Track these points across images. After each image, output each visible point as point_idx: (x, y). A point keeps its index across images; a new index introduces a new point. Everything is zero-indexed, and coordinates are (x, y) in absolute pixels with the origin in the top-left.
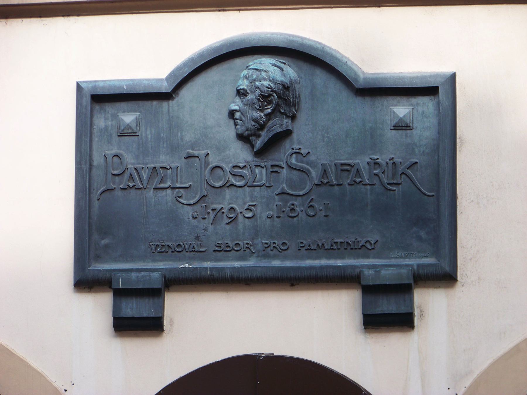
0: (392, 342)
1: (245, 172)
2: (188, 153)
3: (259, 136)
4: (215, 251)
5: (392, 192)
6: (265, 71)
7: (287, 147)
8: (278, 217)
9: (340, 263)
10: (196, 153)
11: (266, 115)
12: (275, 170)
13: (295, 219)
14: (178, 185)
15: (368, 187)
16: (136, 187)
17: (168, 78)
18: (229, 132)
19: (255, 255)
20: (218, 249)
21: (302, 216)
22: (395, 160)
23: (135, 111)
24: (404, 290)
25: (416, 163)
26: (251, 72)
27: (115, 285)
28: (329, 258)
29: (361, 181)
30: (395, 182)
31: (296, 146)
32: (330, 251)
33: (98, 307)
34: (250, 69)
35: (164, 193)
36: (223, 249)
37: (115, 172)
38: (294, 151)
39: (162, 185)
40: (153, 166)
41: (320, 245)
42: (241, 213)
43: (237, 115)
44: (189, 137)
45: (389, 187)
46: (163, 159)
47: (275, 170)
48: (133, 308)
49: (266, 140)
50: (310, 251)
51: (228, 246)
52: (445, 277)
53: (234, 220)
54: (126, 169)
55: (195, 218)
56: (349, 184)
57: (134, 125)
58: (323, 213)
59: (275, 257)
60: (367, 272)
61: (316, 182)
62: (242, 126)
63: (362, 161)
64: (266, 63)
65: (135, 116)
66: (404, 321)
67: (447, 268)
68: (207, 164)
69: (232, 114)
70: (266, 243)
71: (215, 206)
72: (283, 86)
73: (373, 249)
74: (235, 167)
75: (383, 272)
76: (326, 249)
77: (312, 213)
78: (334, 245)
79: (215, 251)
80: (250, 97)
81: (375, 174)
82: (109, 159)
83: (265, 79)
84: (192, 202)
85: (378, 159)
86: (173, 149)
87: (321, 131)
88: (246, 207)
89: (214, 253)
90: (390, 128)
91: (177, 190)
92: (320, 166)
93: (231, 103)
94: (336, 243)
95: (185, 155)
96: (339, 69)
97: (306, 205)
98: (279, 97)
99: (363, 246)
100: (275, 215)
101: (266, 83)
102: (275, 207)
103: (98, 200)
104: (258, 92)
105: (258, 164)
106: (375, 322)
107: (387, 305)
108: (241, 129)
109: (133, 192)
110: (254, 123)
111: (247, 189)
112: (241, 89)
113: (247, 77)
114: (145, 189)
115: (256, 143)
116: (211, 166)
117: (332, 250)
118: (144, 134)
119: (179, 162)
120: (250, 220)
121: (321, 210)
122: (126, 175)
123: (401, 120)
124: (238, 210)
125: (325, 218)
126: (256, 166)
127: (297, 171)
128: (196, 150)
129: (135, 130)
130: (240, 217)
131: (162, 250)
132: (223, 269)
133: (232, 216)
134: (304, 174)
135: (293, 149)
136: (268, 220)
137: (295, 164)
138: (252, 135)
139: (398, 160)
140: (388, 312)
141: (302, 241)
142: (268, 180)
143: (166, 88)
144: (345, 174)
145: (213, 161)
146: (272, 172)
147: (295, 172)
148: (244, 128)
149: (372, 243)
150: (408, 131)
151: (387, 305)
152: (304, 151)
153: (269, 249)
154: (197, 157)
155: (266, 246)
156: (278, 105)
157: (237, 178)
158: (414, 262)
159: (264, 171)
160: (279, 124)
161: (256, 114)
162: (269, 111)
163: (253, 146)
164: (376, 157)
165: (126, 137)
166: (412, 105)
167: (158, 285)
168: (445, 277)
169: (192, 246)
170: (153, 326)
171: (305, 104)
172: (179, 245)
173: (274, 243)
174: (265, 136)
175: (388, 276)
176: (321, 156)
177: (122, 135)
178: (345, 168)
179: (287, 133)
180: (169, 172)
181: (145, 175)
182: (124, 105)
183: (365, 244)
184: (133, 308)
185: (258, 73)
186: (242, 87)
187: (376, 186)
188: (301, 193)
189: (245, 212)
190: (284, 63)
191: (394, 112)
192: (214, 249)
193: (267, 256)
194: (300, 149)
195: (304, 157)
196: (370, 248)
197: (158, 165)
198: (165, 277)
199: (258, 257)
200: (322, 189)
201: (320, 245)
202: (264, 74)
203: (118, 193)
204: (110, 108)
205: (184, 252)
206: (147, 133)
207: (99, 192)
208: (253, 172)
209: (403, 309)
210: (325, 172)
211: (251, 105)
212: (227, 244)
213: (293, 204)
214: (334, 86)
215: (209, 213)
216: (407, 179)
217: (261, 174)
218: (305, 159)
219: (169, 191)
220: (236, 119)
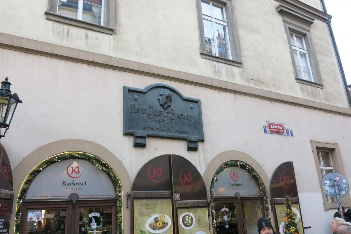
1: (162, 113)
3: (165, 105)
9: (182, 135)
10: (151, 107)
12: (168, 113)
18: (157, 104)
19: (165, 132)
21: (174, 124)
24: (196, 142)
26: (163, 91)
28: (180, 134)
35: (144, 115)
36: (157, 129)
43: (160, 100)
47: (168, 113)
48: (140, 141)
52: (203, 141)
53: (160, 123)
55: (152, 122)
57: (137, 98)
60: (189, 138)
63: (185, 114)
64: (166, 90)
69: (159, 100)
74: (160, 111)
75: (193, 138)
80: (164, 96)
82: (132, 105)
87: (177, 106)
104: (166, 95)
106: (190, 149)
107: (193, 146)
108: (161, 103)
109: (138, 114)
113: (162, 92)
116: (155, 110)
122: (136, 110)
130: (161, 123)
131: (145, 128)
134: (174, 116)
138: (164, 105)
139: (192, 115)
143: (145, 91)
148: (162, 103)
152: (174, 110)
160: (169, 104)
161: (166, 100)
168: (203, 141)
172: (148, 128)
174: (167, 105)
176: (177, 112)
178: (182, 115)
179: (170, 106)
182: (136, 93)
184: (140, 141)
197: (143, 108)
200: (177, 119)
203: (134, 113)
204: (132, 93)
209: (196, 147)
211: (164, 98)
214: (178, 98)
217: (165, 114)
219: (146, 115)
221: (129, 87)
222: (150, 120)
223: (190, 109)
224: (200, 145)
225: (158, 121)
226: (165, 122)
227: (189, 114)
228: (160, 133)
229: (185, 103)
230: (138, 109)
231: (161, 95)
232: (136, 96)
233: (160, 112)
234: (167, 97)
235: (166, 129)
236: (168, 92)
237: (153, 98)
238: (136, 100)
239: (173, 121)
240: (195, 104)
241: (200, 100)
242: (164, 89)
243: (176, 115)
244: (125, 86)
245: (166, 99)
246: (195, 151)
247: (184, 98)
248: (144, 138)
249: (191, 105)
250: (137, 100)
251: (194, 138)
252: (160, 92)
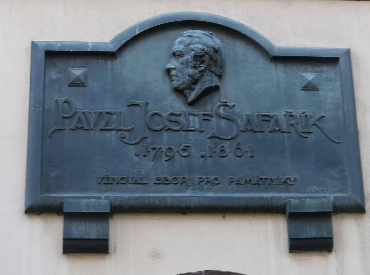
1: (182, 119)
2: (131, 102)
3: (193, 89)
4: (155, 183)
5: (306, 139)
6: (198, 37)
8: (210, 157)
9: (265, 195)
10: (138, 102)
11: (200, 72)
12: (207, 118)
13: (225, 159)
14: (122, 128)
15: (286, 134)
16: (84, 128)
17: (113, 42)
18: (163, 87)
19: (190, 188)
20: (158, 182)
21: (231, 155)
22: (306, 114)
23: (83, 67)
25: (324, 116)
26: (185, 39)
27: (288, 211)
28: (256, 192)
29: (280, 130)
30: (307, 131)
31: (223, 100)
32: (256, 185)
34: (184, 36)
35: (108, 134)
36: (162, 182)
37: (65, 115)
38: (222, 104)
39: (108, 128)
40: (100, 111)
41: (248, 180)
42: (178, 152)
43: (173, 72)
45: (303, 135)
46: (108, 107)
47: (207, 118)
49: (199, 93)
50: (239, 185)
51: (167, 180)
52: (358, 209)
53: (170, 159)
54: (76, 113)
56: (270, 132)
57: (82, 78)
58: (249, 154)
59: (209, 190)
61: (241, 129)
62: (178, 81)
63: (280, 113)
64: (198, 33)
65: (83, 71)
66: (324, 245)
67: (359, 201)
68: (146, 112)
69: (168, 71)
70: (200, 178)
71: (156, 146)
72: (214, 49)
73: (293, 184)
74: (172, 114)
76: (253, 184)
77: (240, 154)
78: (259, 180)
79: (155, 183)
80: (185, 57)
81: (291, 125)
83: (198, 43)
84: (134, 142)
85: (292, 112)
87: (246, 87)
88: (182, 147)
89: (155, 186)
90: (300, 88)
91: (120, 132)
92: (245, 117)
93: (167, 63)
94: (261, 179)
95: (128, 104)
96: (257, 40)
97: (234, 147)
98: (211, 58)
99: (284, 182)
100: (208, 155)
101: (200, 46)
102: (207, 148)
103: (50, 137)
104: (193, 53)
105: (192, 113)
108: (176, 83)
109: (82, 133)
110: (190, 79)
111: (183, 133)
112: (176, 51)
113: (181, 42)
114: (92, 130)
115: (190, 95)
118: (91, 85)
119: (124, 110)
120: (185, 158)
121: (247, 152)
122: (76, 119)
123: (310, 83)
124: (175, 149)
125: (250, 158)
126: (190, 114)
127: (225, 120)
128: (137, 100)
129: (84, 81)
130: (177, 156)
131: (107, 182)
132: (165, 198)
133: (170, 155)
134: (232, 123)
135: (221, 102)
136: (201, 159)
137: (222, 114)
138: (186, 88)
141: (232, 177)
142: (201, 125)
143: (112, 48)
144: (265, 123)
145: (152, 109)
146: (204, 120)
147: (223, 121)
148: (180, 82)
149: (293, 179)
150: (315, 92)
153: (204, 183)
154: (138, 105)
155: (201, 180)
156: (209, 65)
157: (173, 124)
159: (196, 119)
160: (209, 81)
161: (191, 71)
162: (202, 68)
163: (186, 97)
164: (291, 111)
165: (75, 88)
166: (316, 72)
167: (108, 210)
169: (134, 179)
172: (123, 178)
173: (208, 178)
176: (244, 109)
177: (72, 85)
178: (266, 118)
179: (215, 89)
180: (114, 116)
181: (93, 118)
183: (286, 181)
185: (191, 39)
186: (177, 50)
187: (291, 134)
188: (229, 137)
189: (181, 152)
190: (211, 34)
191: (303, 77)
192: (154, 182)
193: (202, 189)
194: (226, 102)
195: (231, 108)
196: (291, 183)
198: (111, 204)
199: (194, 189)
200: (247, 134)
201: (248, 180)
202: (197, 39)
204: (61, 63)
205: (128, 184)
206: (94, 85)
207: (50, 132)
208: (187, 120)
209: (325, 235)
210: (249, 121)
211: (186, 64)
212: (166, 178)
213: (223, 147)
214: (252, 55)
215: (149, 152)
216: (317, 129)
217: (195, 122)
218: (231, 110)
219: (113, 133)
220: (173, 75)
221: (49, 44)
222: (132, 150)
223: (303, 92)
224: (346, 229)
225: (164, 149)
226: (193, 150)
227: (297, 112)
228: (170, 195)
229: (278, 73)
230: (82, 117)
231: (174, 54)
232: (77, 72)
233: (173, 118)
234: (199, 58)
235: (196, 177)
236: (201, 39)
237: (147, 71)
238: (77, 84)
239: (226, 144)
240: (328, 72)
241: (348, 52)
242: (187, 32)
243: (242, 123)
244: (35, 40)
245: (195, 67)
246: (326, 253)
247: (277, 54)
248: (103, 217)
249: (309, 75)
250: (82, 85)
251: (312, 199)
252: (173, 45)
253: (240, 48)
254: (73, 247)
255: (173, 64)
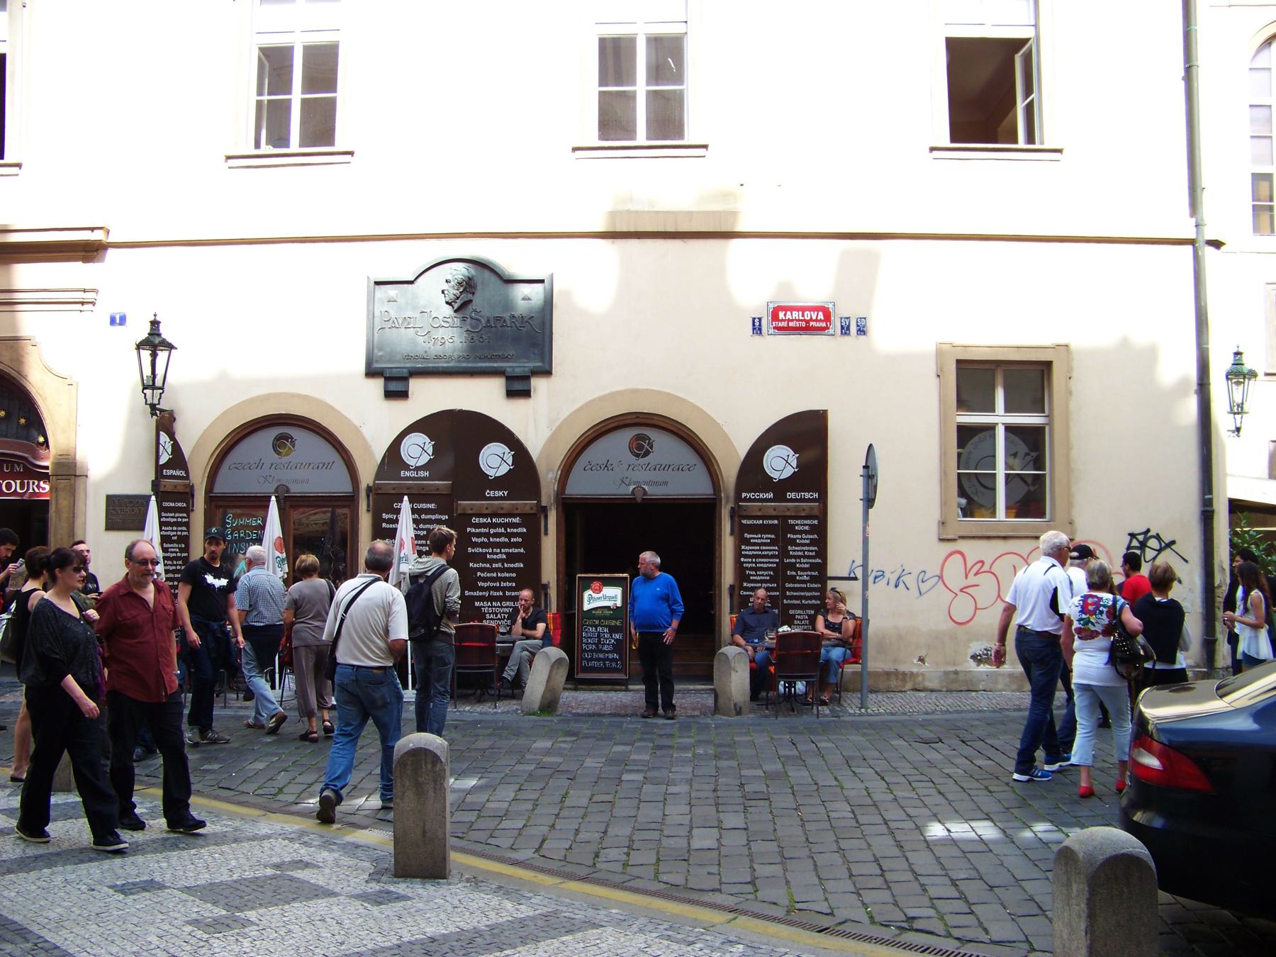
0: (520, 403)
7: (470, 308)
24: (526, 379)
33: (377, 385)
44: (422, 303)
46: (409, 314)
48: (394, 386)
52: (547, 373)
63: (506, 316)
66: (526, 394)
86: (414, 308)
106: (511, 394)
107: (518, 386)
117: (491, 359)
119: (418, 315)
140: (518, 389)
151: (518, 386)
158: (531, 365)
167: (406, 375)
168: (547, 373)
170: (404, 395)
171: (479, 287)
174: (459, 302)
175: (518, 372)
176: (487, 313)
178: (498, 319)
179: (470, 301)
184: (394, 386)
206: (401, 301)
214: (493, 278)
224: (538, 384)
251: (517, 367)
253: (487, 273)
254: (389, 395)
255: (446, 286)
